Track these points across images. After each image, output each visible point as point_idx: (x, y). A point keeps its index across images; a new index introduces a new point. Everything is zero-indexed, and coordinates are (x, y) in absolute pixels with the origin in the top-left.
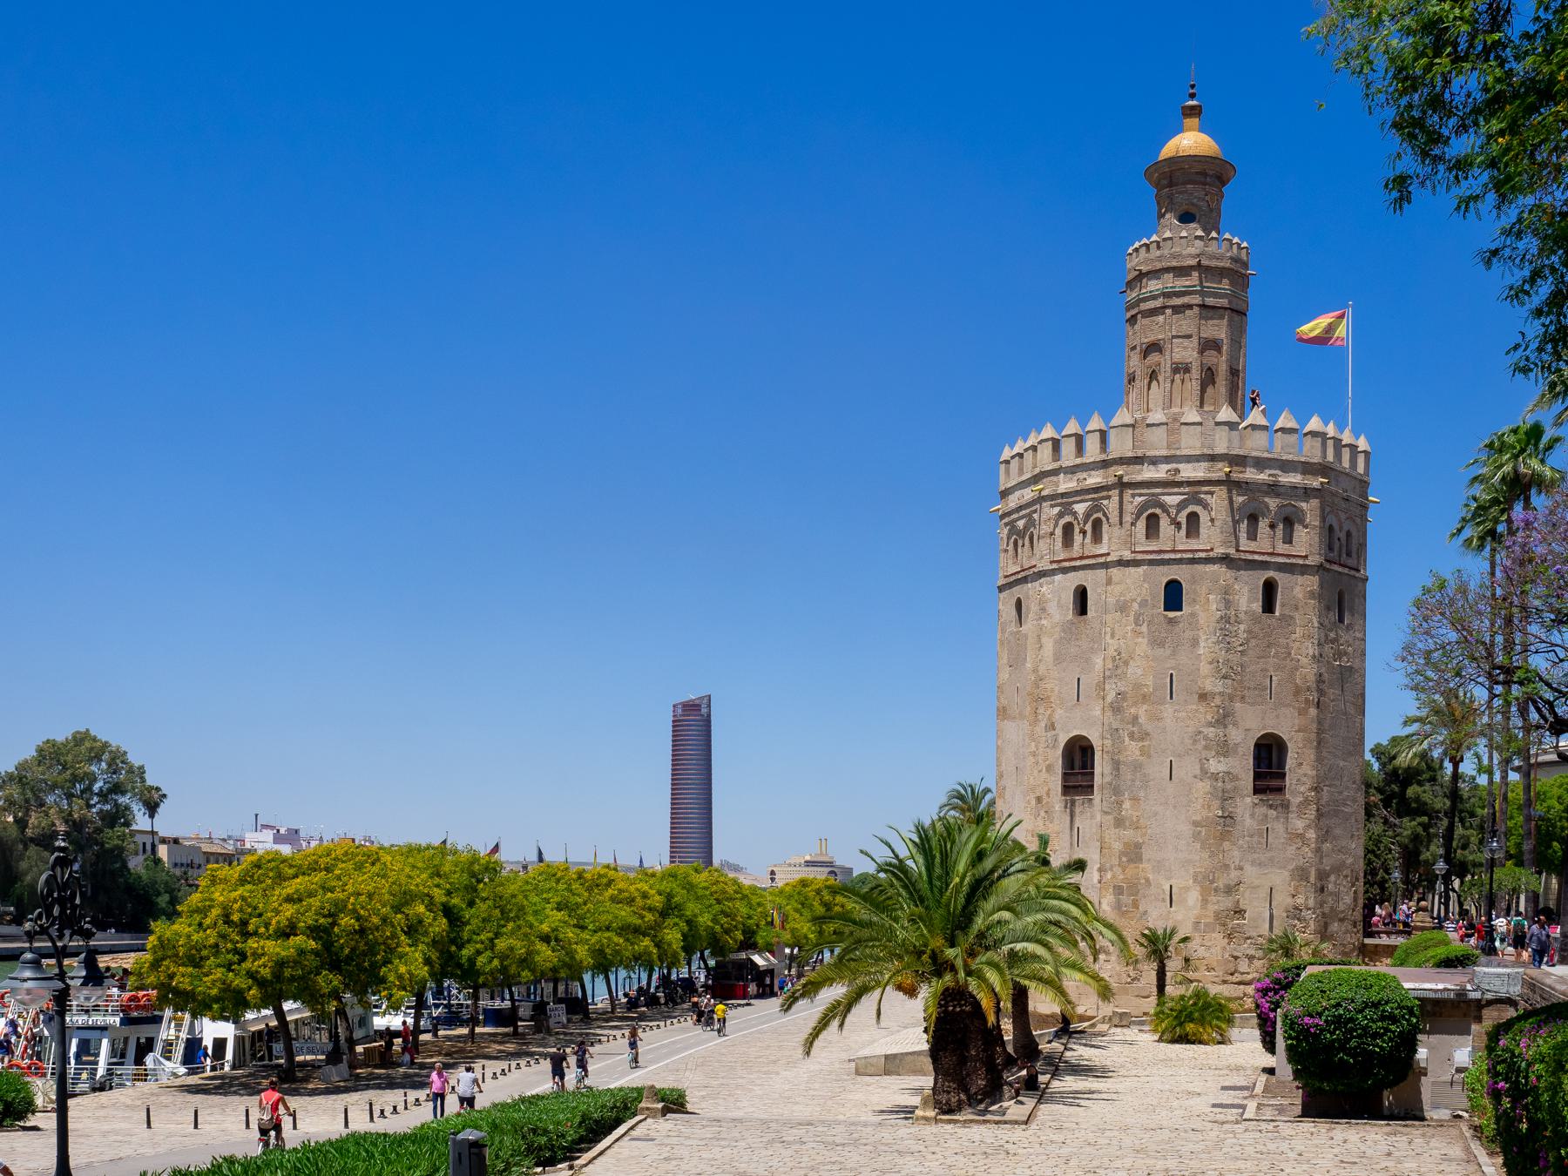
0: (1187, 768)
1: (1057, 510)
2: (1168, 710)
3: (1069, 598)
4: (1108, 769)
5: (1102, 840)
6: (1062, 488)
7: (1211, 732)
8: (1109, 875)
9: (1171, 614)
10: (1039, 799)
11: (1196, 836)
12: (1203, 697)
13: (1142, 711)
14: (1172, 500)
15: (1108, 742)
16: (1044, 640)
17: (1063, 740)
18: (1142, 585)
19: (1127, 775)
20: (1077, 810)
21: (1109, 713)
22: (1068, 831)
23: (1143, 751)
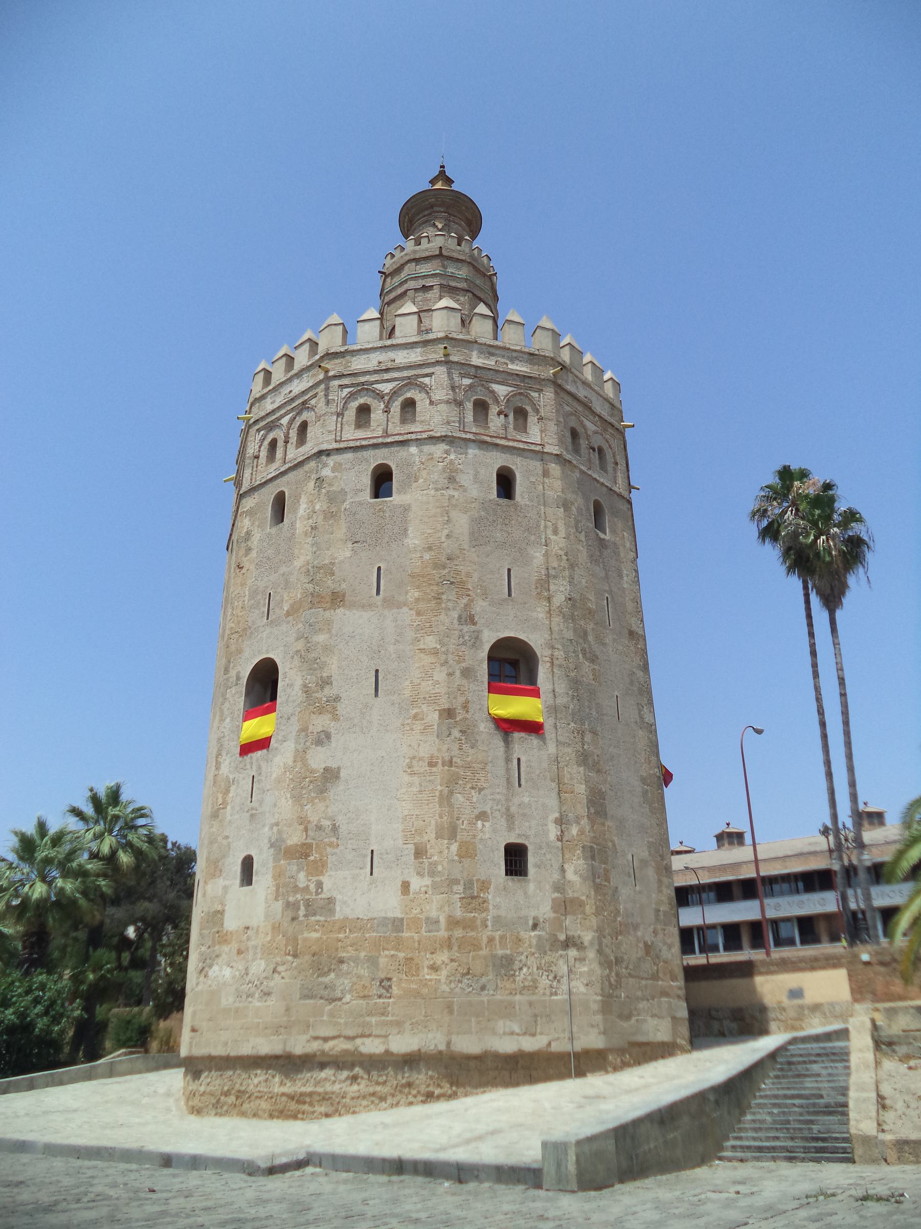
5: (559, 780)
8: (574, 830)
10: (449, 713)
15: (560, 654)
17: (489, 638)
21: (557, 620)
22: (501, 762)
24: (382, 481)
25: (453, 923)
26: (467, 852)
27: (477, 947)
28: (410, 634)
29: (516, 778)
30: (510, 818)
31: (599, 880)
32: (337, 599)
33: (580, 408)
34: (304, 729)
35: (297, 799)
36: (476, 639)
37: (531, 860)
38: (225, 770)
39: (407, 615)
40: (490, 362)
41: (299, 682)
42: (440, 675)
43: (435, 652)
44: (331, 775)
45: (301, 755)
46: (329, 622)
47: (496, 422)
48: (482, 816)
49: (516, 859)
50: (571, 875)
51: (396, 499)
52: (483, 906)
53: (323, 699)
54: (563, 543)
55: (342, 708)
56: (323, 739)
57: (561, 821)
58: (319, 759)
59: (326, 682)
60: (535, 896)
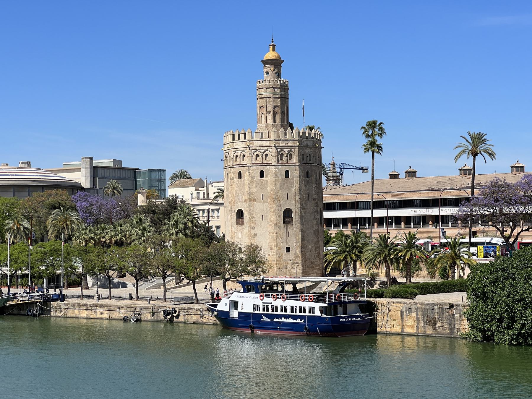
3: (284, 173)
6: (281, 145)
7: (315, 208)
14: (307, 151)
17: (283, 209)
20: (288, 227)
24: (262, 174)
25: (277, 261)
26: (279, 249)
28: (269, 209)
29: (287, 236)
30: (287, 242)
31: (303, 252)
32: (254, 200)
34: (250, 226)
35: (250, 239)
38: (233, 230)
39: (268, 205)
40: (284, 144)
41: (248, 217)
42: (274, 217)
43: (273, 212)
44: (255, 235)
45: (250, 231)
46: (253, 205)
47: (285, 159)
48: (282, 243)
49: (288, 250)
50: (297, 252)
53: (252, 220)
54: (298, 186)
57: (296, 242)
58: (253, 232)
59: (253, 217)
60: (291, 255)
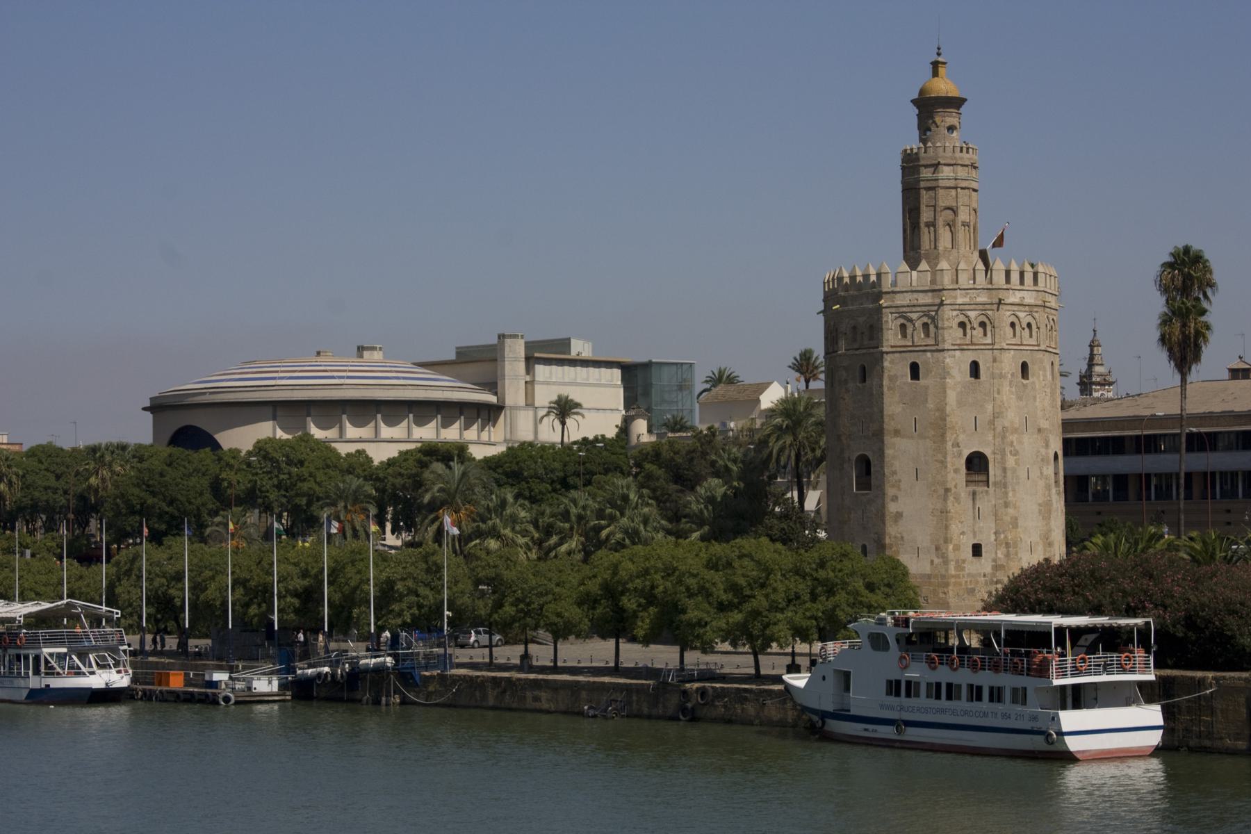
0: (1034, 474)
1: (955, 313)
2: (1026, 438)
3: (967, 368)
4: (999, 472)
6: (960, 301)
9: (1025, 382)
11: (1040, 512)
12: (1039, 430)
13: (1013, 438)
15: (998, 457)
16: (949, 392)
17: (966, 453)
18: (1009, 363)
19: (1009, 474)
23: (1016, 463)
24: (915, 371)
27: (960, 584)
32: (897, 433)
33: (1016, 308)
36: (960, 454)
37: (984, 550)
40: (967, 300)
44: (899, 515)
48: (963, 533)
49: (977, 550)
51: (922, 382)
52: (963, 569)
55: (903, 486)
56: (895, 499)
59: (895, 473)
